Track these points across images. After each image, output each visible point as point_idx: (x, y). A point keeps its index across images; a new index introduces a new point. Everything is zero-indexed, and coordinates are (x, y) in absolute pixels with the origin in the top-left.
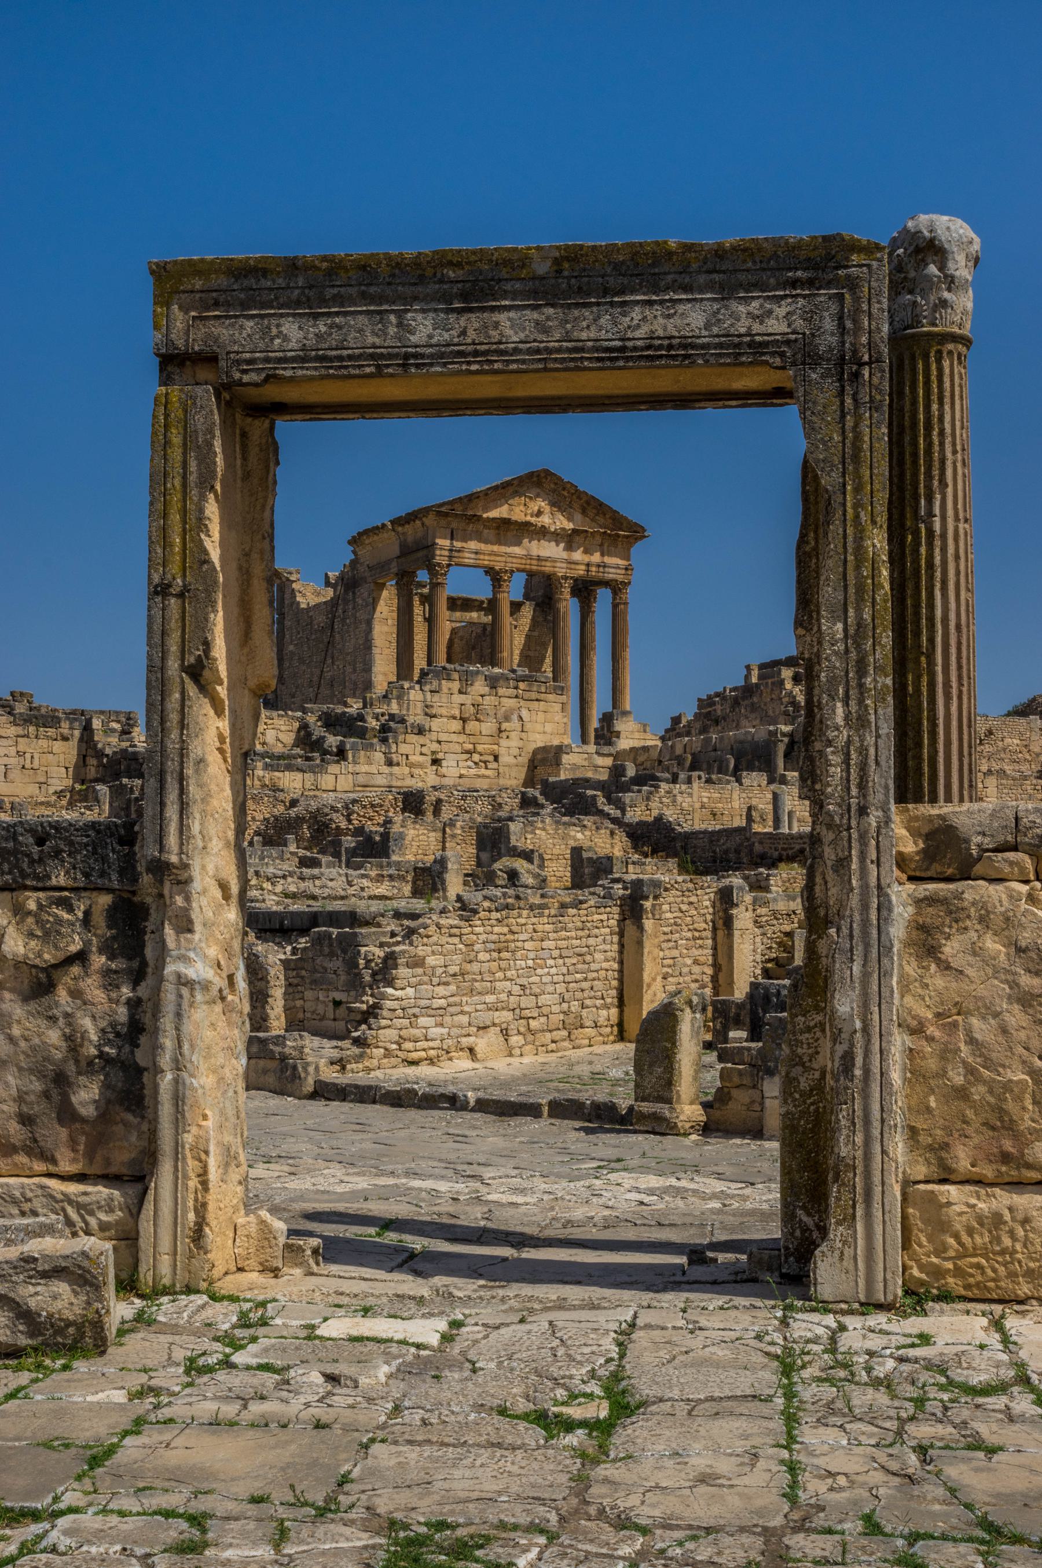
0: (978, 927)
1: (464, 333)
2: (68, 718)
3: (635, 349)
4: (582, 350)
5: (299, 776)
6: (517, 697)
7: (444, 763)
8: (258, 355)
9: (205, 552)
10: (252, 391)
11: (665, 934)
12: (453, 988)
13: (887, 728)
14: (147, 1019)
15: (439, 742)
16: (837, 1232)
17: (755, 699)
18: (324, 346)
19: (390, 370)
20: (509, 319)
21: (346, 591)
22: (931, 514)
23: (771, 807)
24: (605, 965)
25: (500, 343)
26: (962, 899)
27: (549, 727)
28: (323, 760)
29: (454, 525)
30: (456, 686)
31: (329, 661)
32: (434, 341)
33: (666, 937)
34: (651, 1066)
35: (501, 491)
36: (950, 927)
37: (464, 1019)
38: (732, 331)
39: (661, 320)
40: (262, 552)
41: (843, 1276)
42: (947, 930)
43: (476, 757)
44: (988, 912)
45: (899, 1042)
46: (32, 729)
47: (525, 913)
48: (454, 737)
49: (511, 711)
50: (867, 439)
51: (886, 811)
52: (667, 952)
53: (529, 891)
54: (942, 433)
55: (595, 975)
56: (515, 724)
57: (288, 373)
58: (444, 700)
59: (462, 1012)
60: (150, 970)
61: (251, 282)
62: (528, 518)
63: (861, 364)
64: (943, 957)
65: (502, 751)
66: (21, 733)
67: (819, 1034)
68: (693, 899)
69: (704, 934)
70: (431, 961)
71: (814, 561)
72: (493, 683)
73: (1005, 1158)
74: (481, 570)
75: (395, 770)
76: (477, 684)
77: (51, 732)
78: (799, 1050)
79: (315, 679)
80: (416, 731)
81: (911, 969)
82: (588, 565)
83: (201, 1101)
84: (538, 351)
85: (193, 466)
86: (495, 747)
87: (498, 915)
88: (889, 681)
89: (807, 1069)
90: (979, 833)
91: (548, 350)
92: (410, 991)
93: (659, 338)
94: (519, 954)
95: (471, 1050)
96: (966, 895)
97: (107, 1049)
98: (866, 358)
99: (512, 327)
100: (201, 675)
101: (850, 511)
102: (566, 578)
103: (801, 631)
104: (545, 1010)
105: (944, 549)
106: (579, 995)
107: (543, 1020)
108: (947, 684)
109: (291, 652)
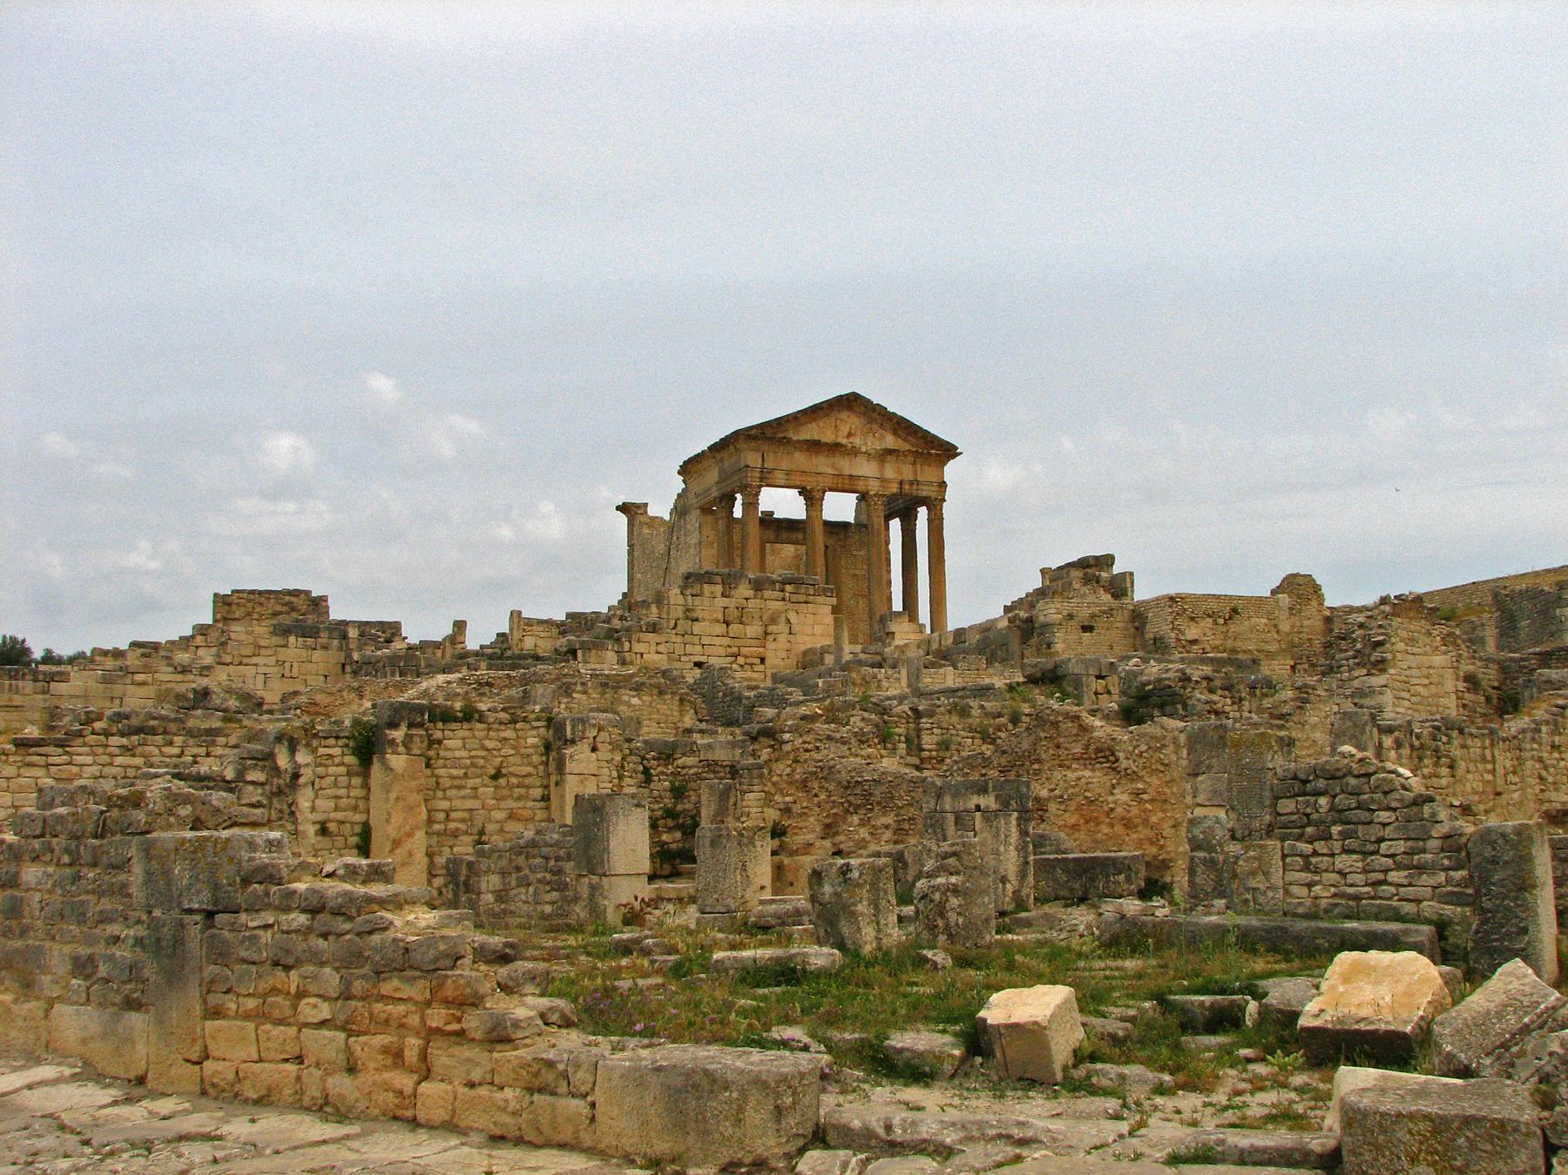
6: (783, 599)
30: (719, 589)
43: (741, 660)
47: (178, 740)
48: (717, 641)
56: (781, 627)
65: (769, 655)
69: (528, 781)
72: (758, 586)
77: (310, 641)
80: (651, 629)
87: (124, 741)
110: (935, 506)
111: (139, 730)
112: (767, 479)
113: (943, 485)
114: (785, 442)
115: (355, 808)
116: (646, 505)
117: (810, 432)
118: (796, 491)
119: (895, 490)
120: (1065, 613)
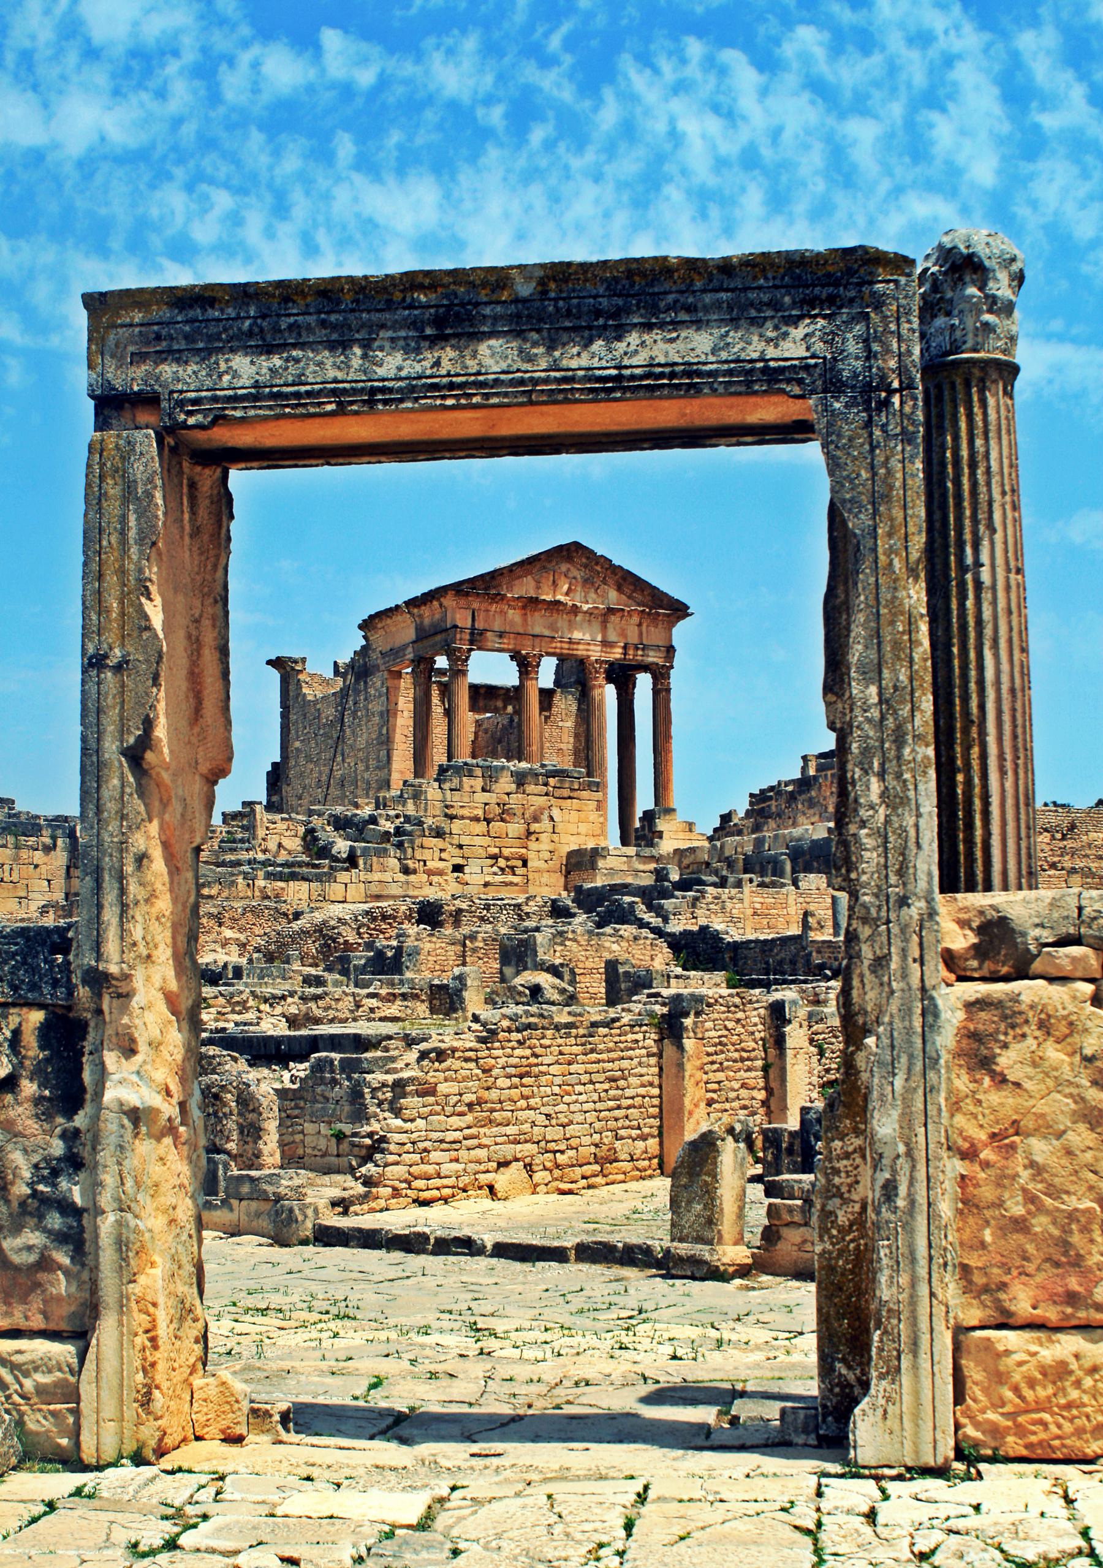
0: (1037, 1033)
1: (437, 364)
3: (633, 377)
4: (572, 380)
5: (305, 885)
6: (547, 794)
7: (467, 870)
8: (204, 394)
9: (147, 618)
10: (201, 435)
11: (708, 1054)
12: (469, 1118)
13: (929, 805)
14: (85, 1153)
15: (460, 847)
16: (878, 1387)
17: (813, 793)
18: (278, 382)
19: (355, 407)
20: (490, 347)
21: (357, 681)
22: (978, 564)
23: (830, 912)
24: (642, 1091)
25: (479, 373)
26: (1018, 1002)
27: (583, 828)
29: (476, 605)
30: (478, 783)
31: (339, 759)
32: (403, 374)
33: (710, 1059)
34: (689, 1202)
35: (527, 567)
36: (1006, 1034)
37: (482, 1153)
38: (743, 356)
39: (660, 344)
40: (214, 618)
41: (887, 1436)
42: (1002, 1037)
43: (502, 863)
44: (1049, 1016)
47: (549, 1033)
48: (478, 841)
49: (541, 810)
50: (899, 475)
51: (930, 901)
52: (711, 1075)
53: (554, 1008)
55: (630, 1102)
56: (545, 825)
57: (238, 414)
58: (466, 799)
59: (480, 1146)
60: (88, 1097)
61: (198, 312)
63: (891, 392)
64: (998, 1069)
65: (531, 855)
67: (858, 1161)
68: (740, 1015)
69: (753, 1054)
70: (442, 1088)
71: (844, 617)
72: (520, 779)
73: (1072, 1298)
74: (506, 656)
75: (412, 878)
76: (502, 780)
78: (837, 1180)
79: (324, 778)
81: (962, 1083)
83: (149, 1245)
84: (522, 382)
86: (523, 851)
87: (519, 1036)
88: (931, 752)
89: (846, 1201)
90: (1037, 925)
91: (535, 382)
92: (420, 1123)
93: (659, 365)
94: (543, 1080)
95: (491, 1188)
96: (1022, 998)
97: (41, 1187)
98: (896, 385)
99: (492, 355)
100: (142, 758)
101: (882, 558)
103: (831, 698)
104: (574, 1142)
105: (994, 603)
106: (612, 1124)
107: (572, 1153)
109: (297, 749)
111: (529, 1026)
112: (477, 639)
113: (670, 650)
114: (499, 598)
115: (651, 1084)
116: (304, 660)
117: (525, 587)
118: (506, 656)
119: (618, 656)
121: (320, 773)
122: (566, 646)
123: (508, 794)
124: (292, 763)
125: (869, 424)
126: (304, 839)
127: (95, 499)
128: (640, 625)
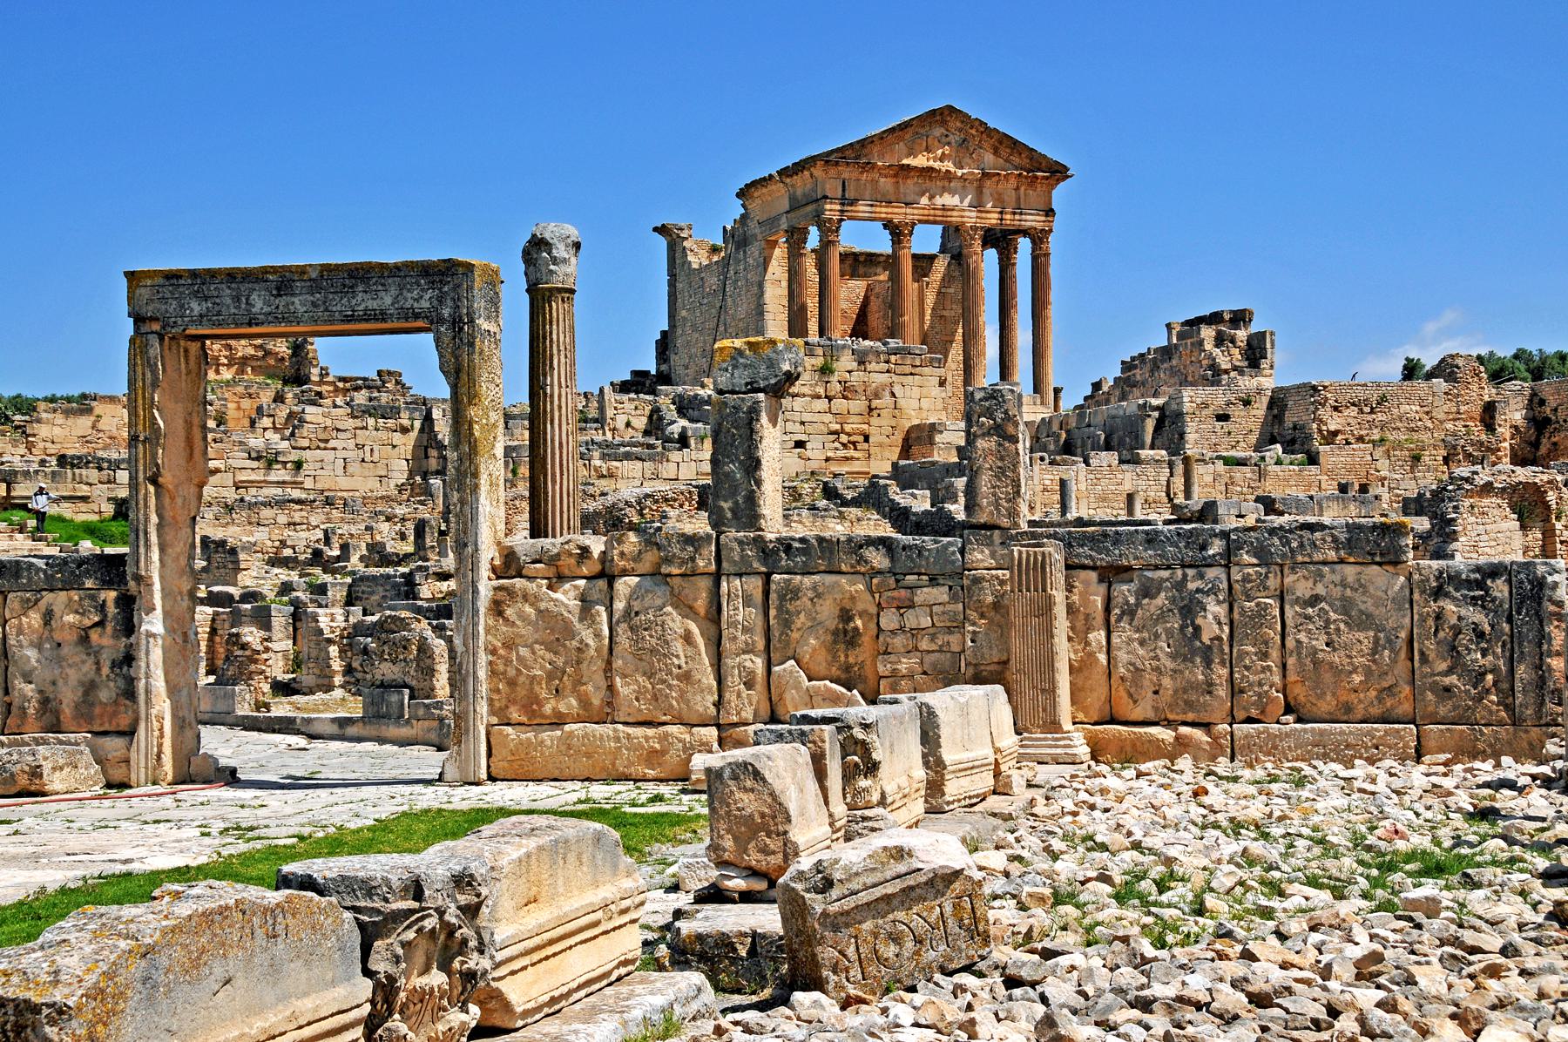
1: (277, 307)
2: (406, 409)
5: (639, 464)
6: (888, 371)
7: (808, 445)
15: (803, 423)
17: (1174, 362)
21: (737, 249)
23: (1057, 497)
28: (664, 448)
29: (846, 175)
31: (722, 328)
45: (483, 658)
46: (371, 422)
48: (816, 418)
54: (551, 341)
56: (887, 400)
61: (175, 281)
62: (931, 163)
65: (873, 431)
66: (360, 425)
74: (879, 225)
76: (842, 359)
77: (391, 423)
82: (1001, 213)
85: (148, 375)
86: (866, 426)
102: (974, 228)
105: (552, 403)
108: (554, 475)
109: (684, 318)
110: (1039, 239)
114: (869, 166)
119: (994, 222)
120: (1199, 401)
121: (705, 342)
122: (940, 213)
123: (849, 372)
124: (679, 331)
125: (454, 338)
126: (650, 417)
127: (132, 366)
128: (1017, 189)
